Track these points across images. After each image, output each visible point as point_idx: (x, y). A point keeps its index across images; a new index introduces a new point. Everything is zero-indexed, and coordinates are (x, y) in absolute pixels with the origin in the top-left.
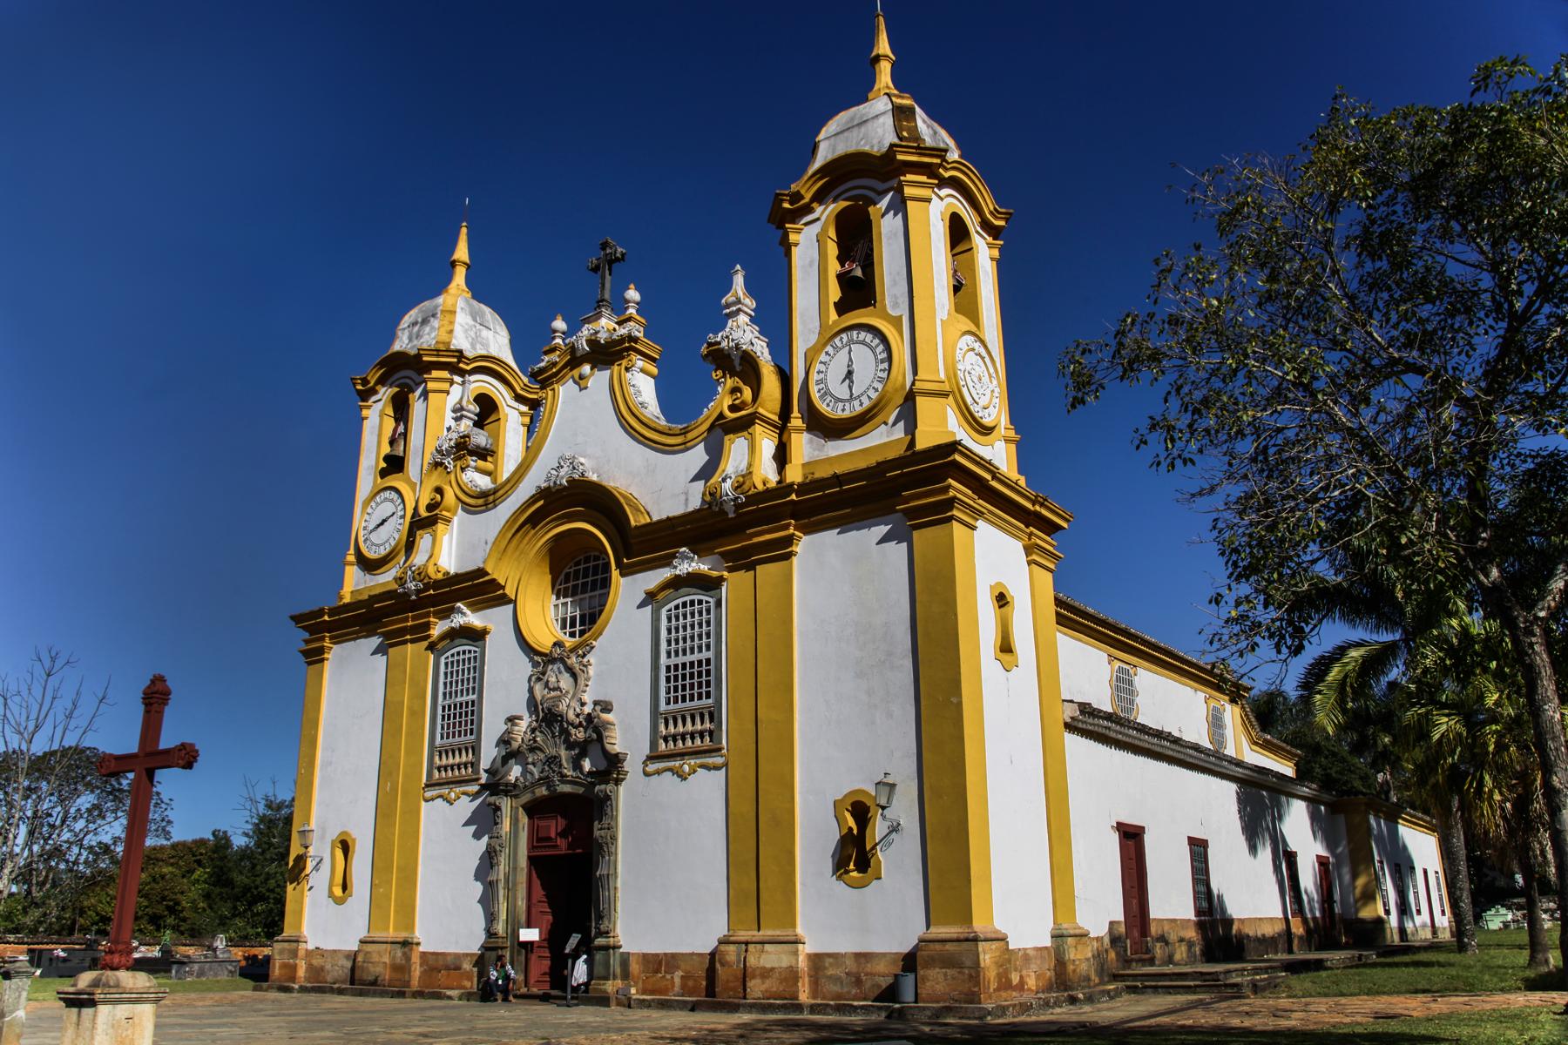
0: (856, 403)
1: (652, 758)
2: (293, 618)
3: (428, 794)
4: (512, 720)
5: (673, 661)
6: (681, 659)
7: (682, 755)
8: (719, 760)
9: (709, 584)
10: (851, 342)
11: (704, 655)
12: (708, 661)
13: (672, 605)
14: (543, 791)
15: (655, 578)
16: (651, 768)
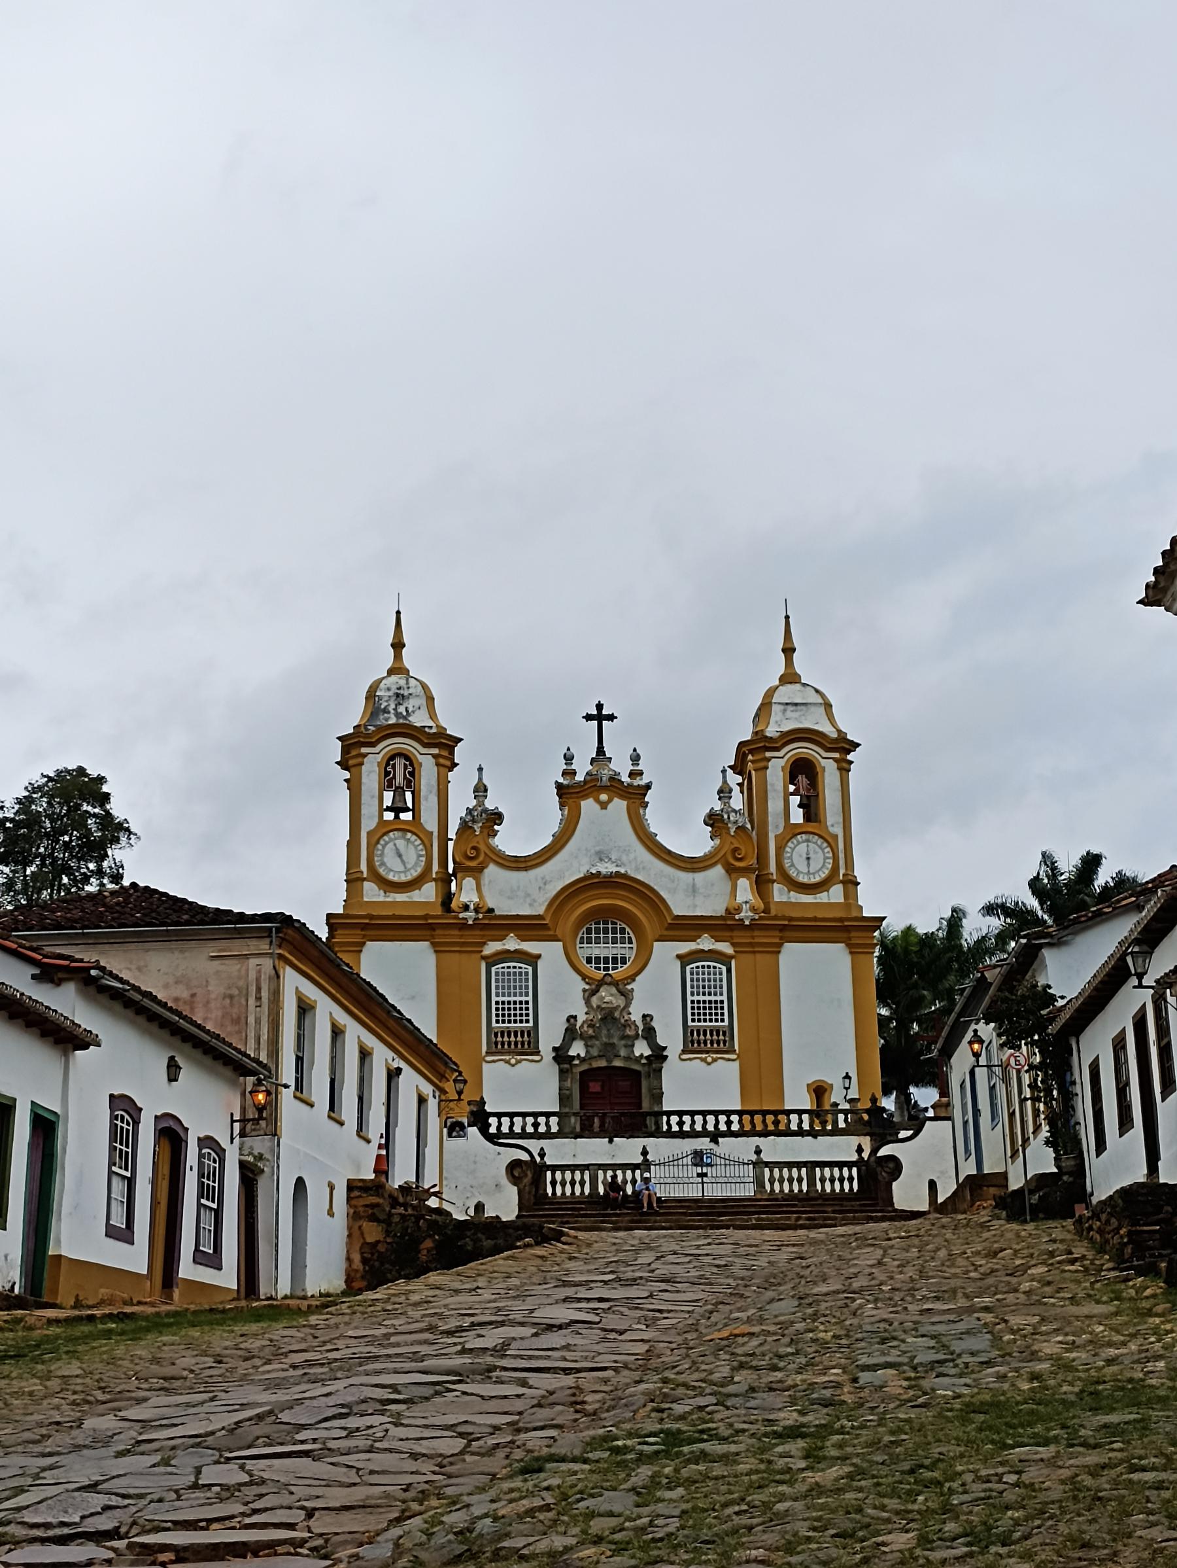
1: (684, 1052)
3: (488, 1058)
4: (572, 1018)
5: (696, 998)
6: (701, 998)
7: (707, 1052)
8: (734, 1057)
9: (724, 959)
10: (808, 841)
11: (719, 998)
12: (722, 1002)
14: (595, 1064)
15: (685, 947)
16: (684, 1057)
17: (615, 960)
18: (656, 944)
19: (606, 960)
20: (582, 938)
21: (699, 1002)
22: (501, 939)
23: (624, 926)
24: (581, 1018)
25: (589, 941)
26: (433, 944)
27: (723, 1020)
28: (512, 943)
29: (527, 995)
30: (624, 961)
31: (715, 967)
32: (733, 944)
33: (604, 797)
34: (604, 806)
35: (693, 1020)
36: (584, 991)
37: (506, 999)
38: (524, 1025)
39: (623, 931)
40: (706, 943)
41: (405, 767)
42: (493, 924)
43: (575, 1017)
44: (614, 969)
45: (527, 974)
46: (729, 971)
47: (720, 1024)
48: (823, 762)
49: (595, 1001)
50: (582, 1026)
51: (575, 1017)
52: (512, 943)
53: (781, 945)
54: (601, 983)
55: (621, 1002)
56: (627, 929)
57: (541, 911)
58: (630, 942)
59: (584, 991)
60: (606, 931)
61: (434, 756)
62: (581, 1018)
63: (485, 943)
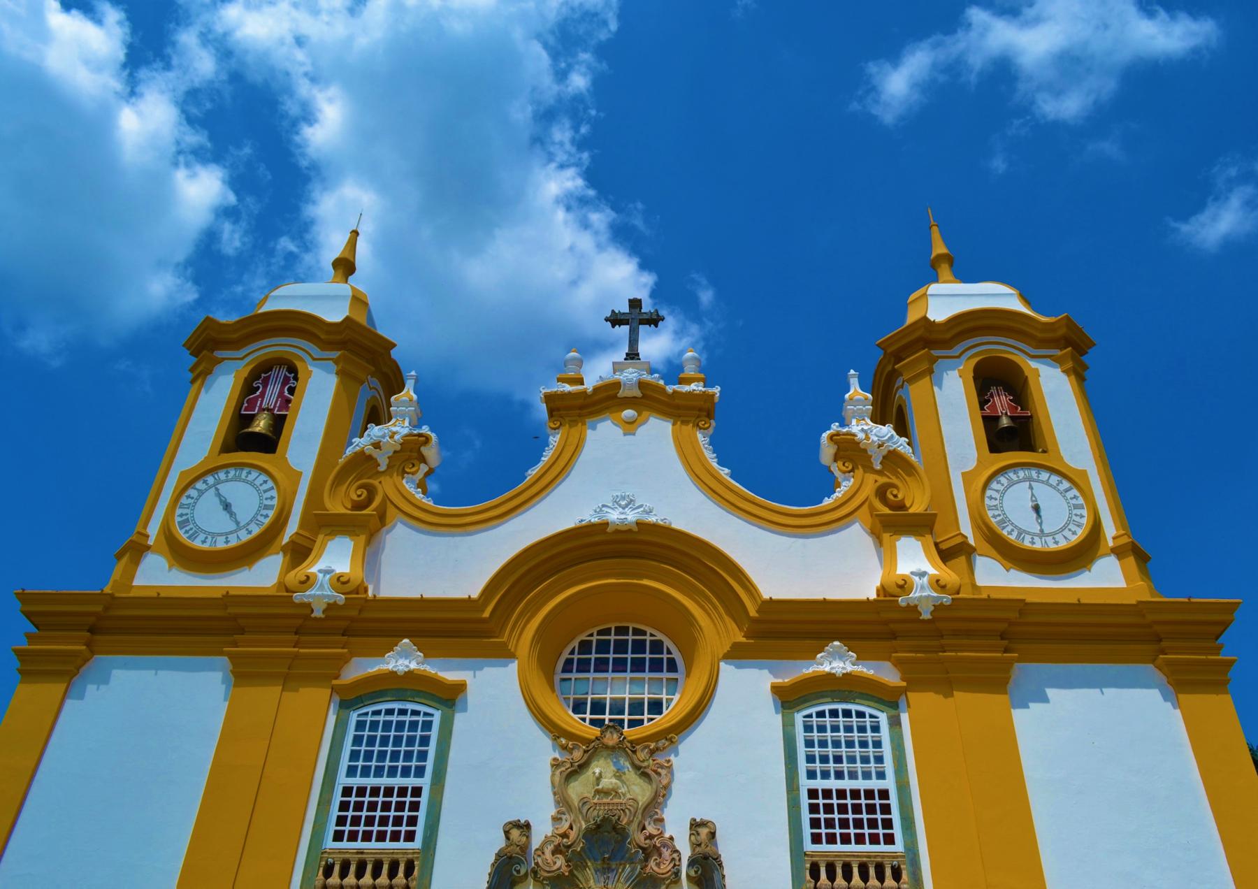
0: (1049, 540)
2: (23, 597)
5: (819, 784)
6: (833, 784)
10: (1030, 479)
11: (875, 784)
13: (813, 710)
17: (636, 707)
18: (726, 669)
19: (617, 708)
20: (569, 662)
21: (827, 794)
22: (381, 652)
23: (659, 636)
24: (542, 830)
25: (583, 666)
26: (232, 657)
27: (890, 840)
28: (403, 660)
29: (420, 772)
30: (656, 707)
31: (860, 714)
32: (898, 664)
33: (629, 413)
34: (630, 427)
35: (816, 839)
36: (555, 759)
37: (370, 781)
38: (401, 844)
39: (657, 646)
40: (835, 662)
41: (286, 381)
42: (367, 620)
43: (526, 827)
44: (633, 724)
45: (428, 725)
46: (895, 723)
47: (882, 848)
48: (1033, 364)
49: (579, 789)
50: (541, 850)
51: (526, 827)
52: (403, 660)
53: (1010, 663)
54: (594, 749)
55: (639, 791)
56: (668, 643)
57: (475, 594)
58: (672, 666)
59: (556, 765)
60: (621, 647)
61: (336, 362)
62: (542, 830)
63: (344, 660)
